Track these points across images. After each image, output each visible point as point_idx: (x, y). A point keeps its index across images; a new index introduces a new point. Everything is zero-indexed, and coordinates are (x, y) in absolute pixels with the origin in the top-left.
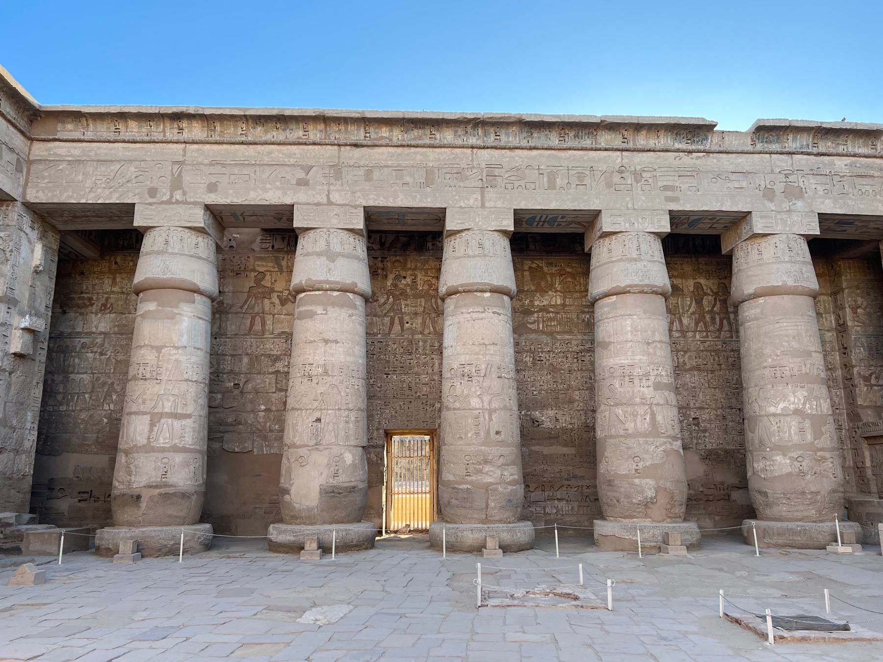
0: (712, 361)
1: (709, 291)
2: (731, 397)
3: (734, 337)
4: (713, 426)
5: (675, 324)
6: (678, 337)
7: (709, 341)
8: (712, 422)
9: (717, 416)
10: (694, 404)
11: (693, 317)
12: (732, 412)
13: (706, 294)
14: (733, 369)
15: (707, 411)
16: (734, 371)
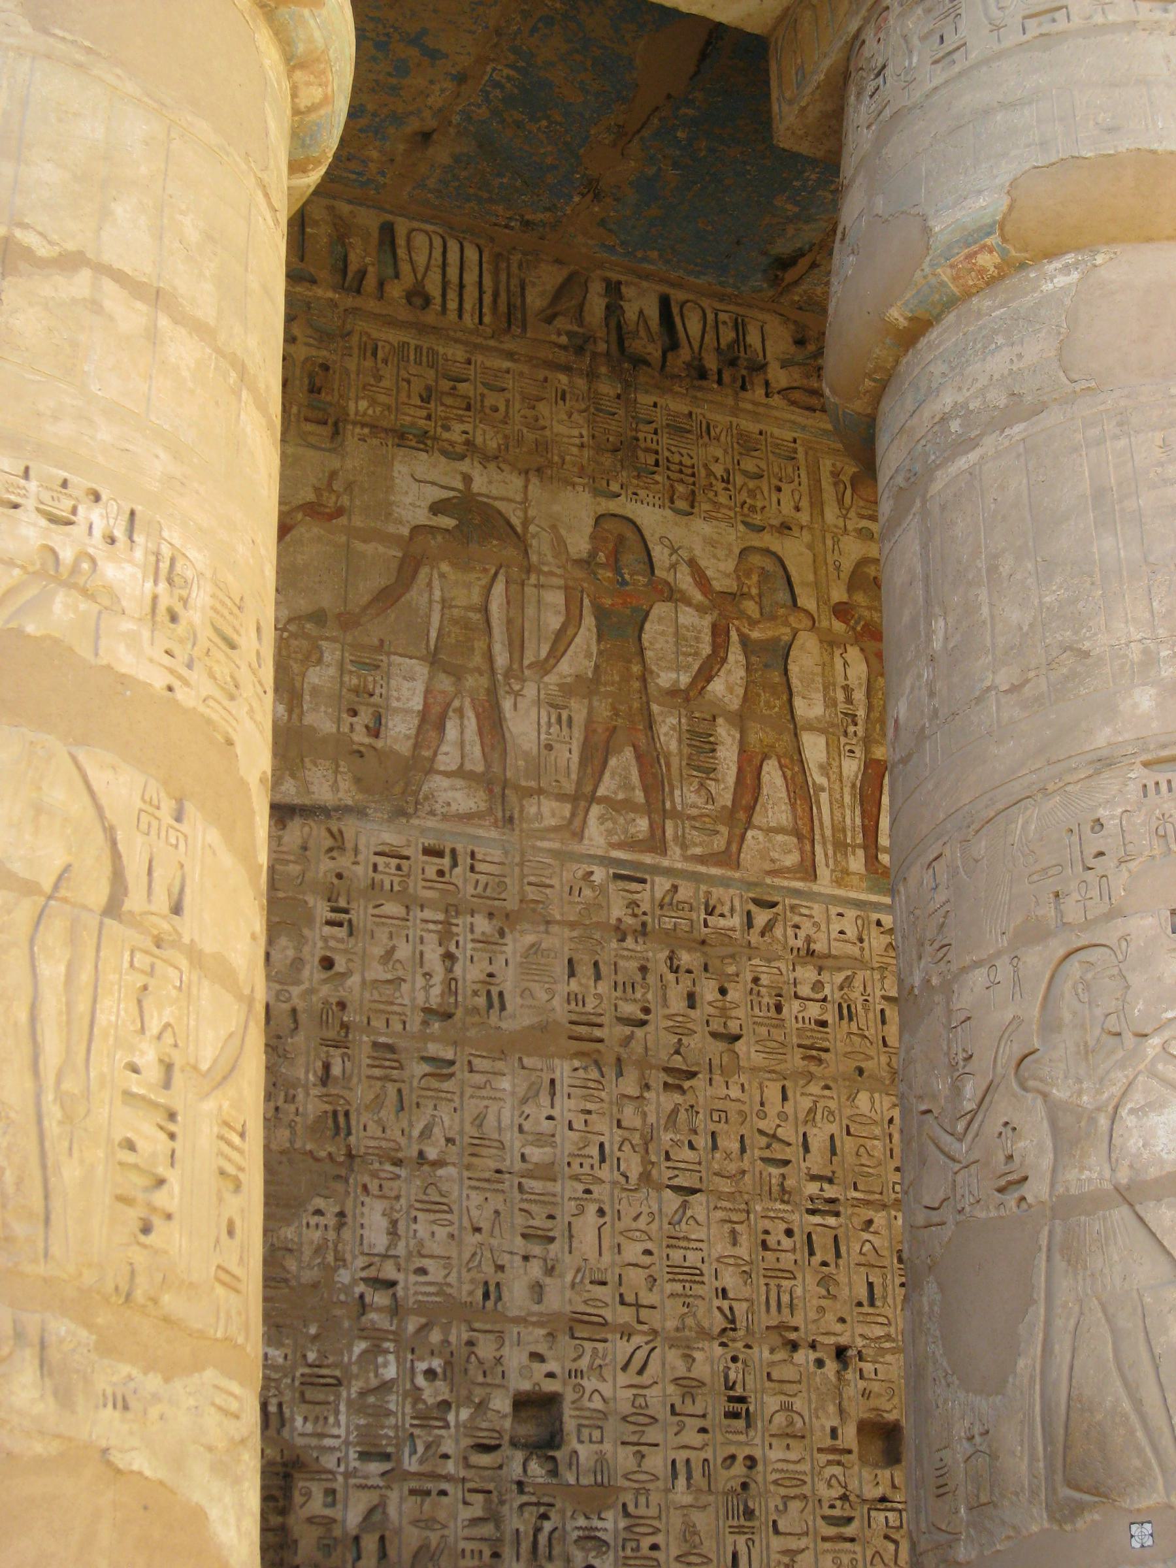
0: (677, 1004)
1: (684, 580)
2: (787, 1260)
3: (823, 872)
4: (656, 1462)
5: (452, 732)
6: (468, 817)
7: (668, 872)
8: (652, 1434)
9: (689, 1387)
10: (538, 1290)
11: (578, 710)
12: (788, 1373)
13: (672, 594)
14: (811, 1077)
15: (623, 1348)
16: (815, 1089)
